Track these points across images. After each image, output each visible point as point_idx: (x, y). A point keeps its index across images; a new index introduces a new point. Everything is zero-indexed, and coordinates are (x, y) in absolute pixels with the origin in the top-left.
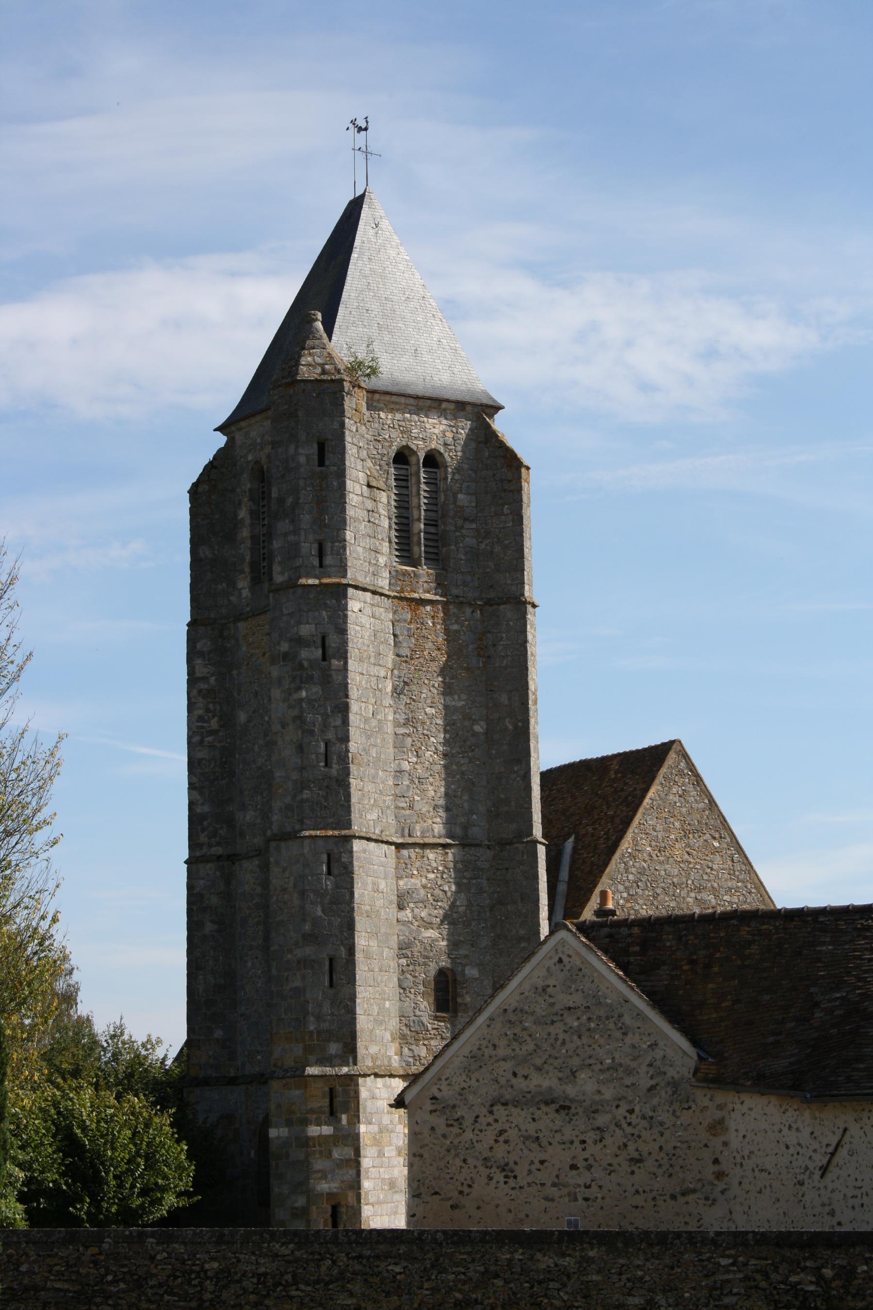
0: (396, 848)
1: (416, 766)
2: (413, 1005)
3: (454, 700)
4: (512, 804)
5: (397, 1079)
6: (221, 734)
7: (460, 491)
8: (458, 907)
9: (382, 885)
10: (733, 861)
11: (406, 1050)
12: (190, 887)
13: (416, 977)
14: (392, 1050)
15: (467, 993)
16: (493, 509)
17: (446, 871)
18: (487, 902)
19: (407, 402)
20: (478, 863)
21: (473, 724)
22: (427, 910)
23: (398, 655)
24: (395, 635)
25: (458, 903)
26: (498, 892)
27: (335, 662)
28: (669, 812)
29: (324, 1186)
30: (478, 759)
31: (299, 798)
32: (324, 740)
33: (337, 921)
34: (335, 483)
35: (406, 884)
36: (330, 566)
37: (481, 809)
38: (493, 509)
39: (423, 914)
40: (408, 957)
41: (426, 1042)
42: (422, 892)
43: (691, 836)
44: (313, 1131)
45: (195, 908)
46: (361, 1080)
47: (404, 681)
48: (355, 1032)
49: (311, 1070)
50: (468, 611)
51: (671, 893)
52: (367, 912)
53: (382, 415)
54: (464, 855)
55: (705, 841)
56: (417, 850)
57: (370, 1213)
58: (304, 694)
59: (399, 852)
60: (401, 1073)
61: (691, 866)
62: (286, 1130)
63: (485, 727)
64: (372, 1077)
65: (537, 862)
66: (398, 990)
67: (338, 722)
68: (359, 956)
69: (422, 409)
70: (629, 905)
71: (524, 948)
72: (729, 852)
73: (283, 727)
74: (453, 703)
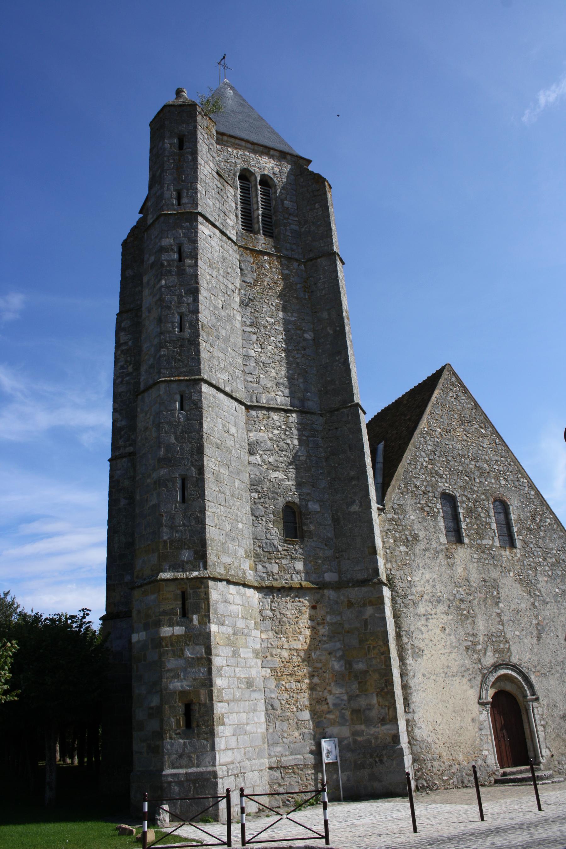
0: (246, 409)
1: (261, 355)
2: (265, 530)
3: (288, 316)
4: (337, 382)
5: (252, 590)
6: (134, 374)
8: (299, 456)
9: (233, 430)
10: (495, 443)
11: (260, 567)
12: (111, 477)
13: (266, 508)
14: (247, 565)
15: (311, 523)
16: (308, 207)
17: (288, 429)
18: (323, 454)
20: (314, 426)
21: (303, 333)
22: (273, 457)
23: (244, 281)
25: (299, 454)
27: (188, 261)
28: (449, 407)
29: (177, 685)
30: (309, 356)
31: (158, 356)
32: (178, 313)
33: (188, 447)
34: (190, 158)
35: (255, 436)
36: (185, 204)
37: (313, 389)
38: (308, 207)
39: (270, 460)
40: (259, 492)
41: (278, 561)
42: (269, 443)
43: (466, 424)
44: (166, 631)
45: (114, 490)
46: (211, 583)
48: (205, 540)
49: (163, 576)
50: (295, 264)
51: (458, 461)
52: (217, 444)
53: (229, 149)
54: (302, 419)
55: (476, 428)
56: (263, 412)
57: (224, 711)
58: (163, 282)
59: (249, 412)
60: (256, 584)
61: (469, 444)
62: (144, 633)
63: (313, 336)
64: (225, 583)
65: (360, 420)
66: (251, 517)
67: (190, 300)
68: (209, 476)
70: (430, 466)
71: (355, 485)
72: (493, 437)
73: (149, 312)
74: (288, 318)
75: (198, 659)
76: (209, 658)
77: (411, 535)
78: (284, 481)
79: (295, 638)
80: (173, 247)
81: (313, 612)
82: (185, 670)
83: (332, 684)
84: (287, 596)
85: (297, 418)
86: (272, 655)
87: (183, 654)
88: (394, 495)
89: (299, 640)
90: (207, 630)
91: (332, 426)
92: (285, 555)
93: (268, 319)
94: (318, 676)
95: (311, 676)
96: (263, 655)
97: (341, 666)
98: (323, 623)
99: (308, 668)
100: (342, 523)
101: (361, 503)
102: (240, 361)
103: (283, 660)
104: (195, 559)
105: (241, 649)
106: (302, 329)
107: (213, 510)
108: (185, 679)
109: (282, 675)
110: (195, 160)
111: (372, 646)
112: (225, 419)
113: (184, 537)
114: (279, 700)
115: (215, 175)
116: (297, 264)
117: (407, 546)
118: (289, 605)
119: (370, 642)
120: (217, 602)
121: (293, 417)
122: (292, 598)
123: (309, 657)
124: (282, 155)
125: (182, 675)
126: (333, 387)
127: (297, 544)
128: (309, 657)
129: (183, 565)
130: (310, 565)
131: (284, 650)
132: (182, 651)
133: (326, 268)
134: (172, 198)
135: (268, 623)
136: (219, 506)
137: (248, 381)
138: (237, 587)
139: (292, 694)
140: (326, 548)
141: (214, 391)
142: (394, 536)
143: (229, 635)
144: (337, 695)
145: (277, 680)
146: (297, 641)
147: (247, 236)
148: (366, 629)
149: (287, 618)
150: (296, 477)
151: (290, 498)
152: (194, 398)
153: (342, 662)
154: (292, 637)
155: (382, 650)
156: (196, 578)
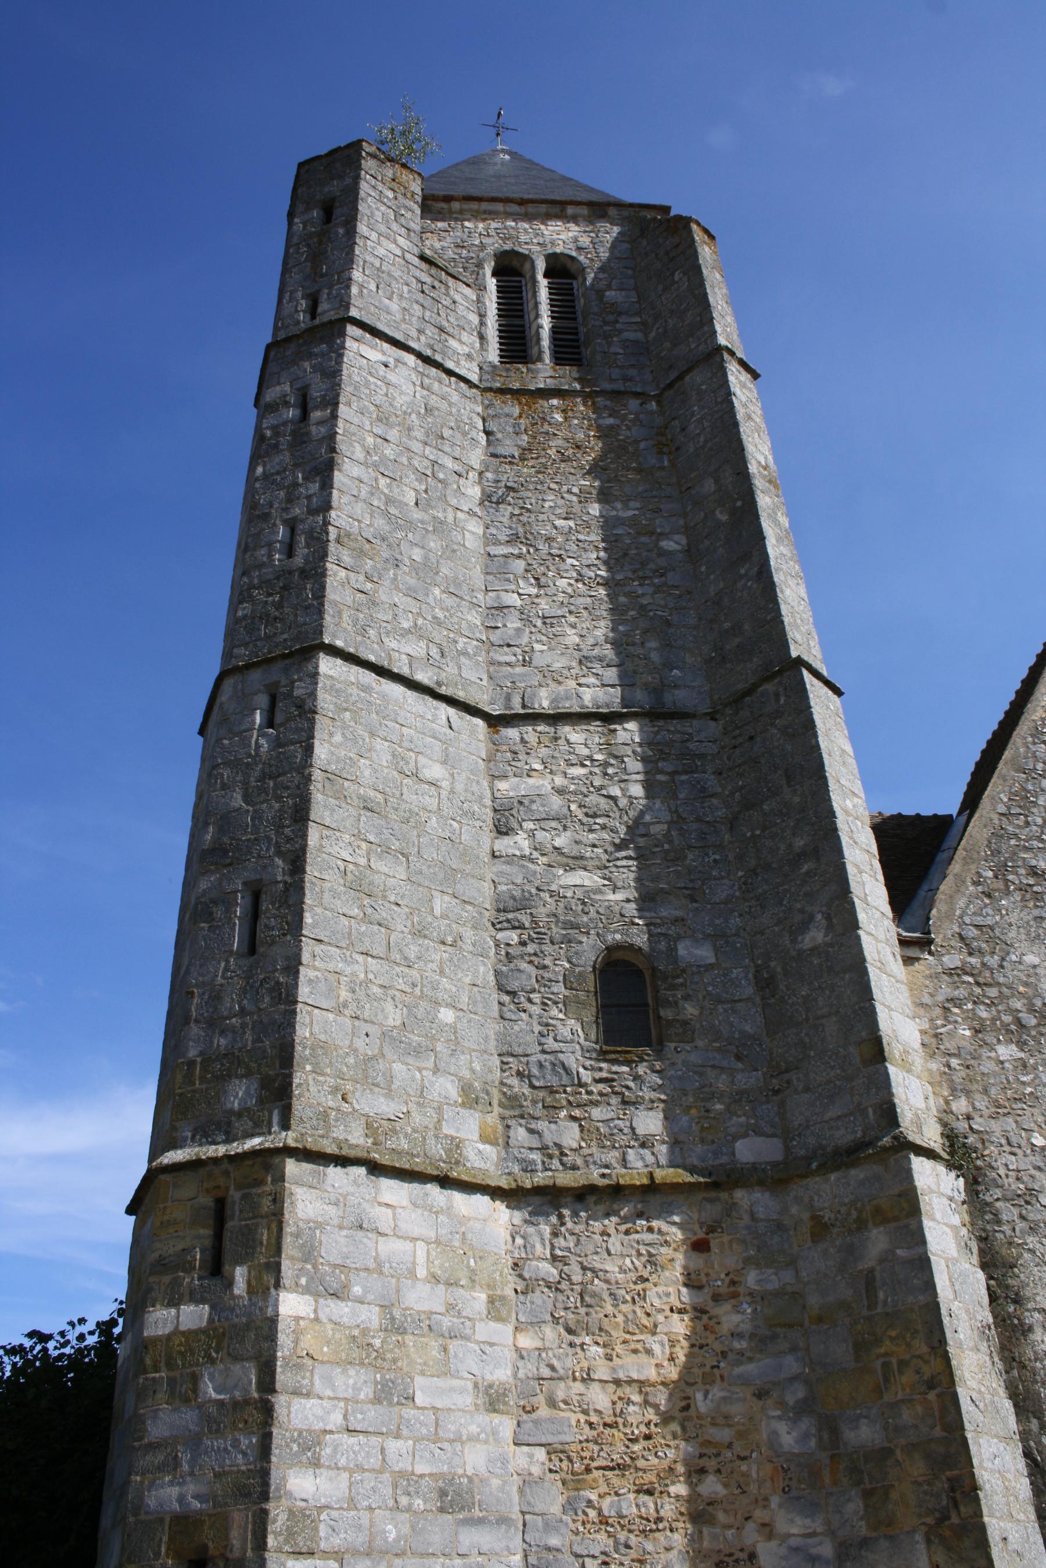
0: (490, 726)
1: (536, 600)
2: (537, 1028)
3: (614, 508)
4: (746, 627)
5: (482, 1201)
7: (609, 287)
8: (647, 825)
11: (520, 1134)
13: (545, 967)
15: (686, 998)
17: (612, 761)
19: (508, 209)
20: (691, 746)
21: (658, 541)
22: (568, 833)
23: (494, 455)
24: (488, 433)
25: (648, 818)
26: (742, 788)
27: (316, 415)
29: (167, 1495)
32: (285, 522)
33: (270, 809)
34: (341, 231)
38: (660, 287)
39: (558, 842)
40: (522, 927)
41: (577, 1113)
42: (556, 802)
46: (291, 1167)
47: (506, 487)
50: (634, 404)
53: (467, 224)
54: (656, 733)
59: (497, 732)
60: (504, 1183)
63: (684, 541)
67: (314, 487)
69: (535, 219)
71: (807, 873)
74: (614, 513)
75: (236, 1405)
76: (268, 1401)
77: (1031, 1010)
78: (601, 892)
79: (633, 1346)
80: (288, 399)
81: (698, 1261)
82: (194, 1442)
83: (775, 1501)
84: (607, 1215)
85: (641, 730)
86: (552, 1403)
87: (195, 1390)
88: (962, 903)
89: (649, 1352)
90: (270, 1312)
91: (740, 735)
92: (601, 1094)
93: (559, 523)
94: (719, 1471)
95: (696, 1473)
96: (517, 1401)
97: (805, 1437)
98: (735, 1295)
99: (683, 1444)
100: (782, 987)
101: (828, 918)
102: (475, 618)
103: (594, 1418)
104: (261, 1101)
105: (419, 1380)
106: (652, 533)
107: (331, 966)
108: (192, 1473)
109: (588, 1470)
110: (351, 232)
111: (894, 1361)
112: (406, 744)
113: (240, 1045)
114: (577, 1556)
115: (416, 261)
116: (638, 402)
117: (1021, 1045)
118: (615, 1243)
119: (887, 1346)
120: (320, 1225)
121: (630, 732)
122: (625, 1220)
123: (686, 1408)
124: (598, 209)
125: (185, 1457)
126: (737, 640)
127: (642, 1060)
128: (686, 1408)
129: (229, 1124)
130: (685, 1118)
131: (596, 1387)
132: (195, 1379)
133: (704, 387)
134: (297, 311)
135: (542, 1298)
136: (360, 958)
137: (500, 664)
138: (416, 1187)
139: (622, 1536)
140: (740, 1065)
141: (368, 677)
142: (971, 1016)
143: (365, 1332)
144: (793, 1542)
145: (571, 1485)
146: (643, 1358)
147: (508, 370)
148: (872, 1305)
149: (607, 1282)
150: (638, 880)
151: (618, 937)
152: (300, 690)
153: (806, 1424)
154: (624, 1342)
155: (927, 1371)
156: (254, 1153)
